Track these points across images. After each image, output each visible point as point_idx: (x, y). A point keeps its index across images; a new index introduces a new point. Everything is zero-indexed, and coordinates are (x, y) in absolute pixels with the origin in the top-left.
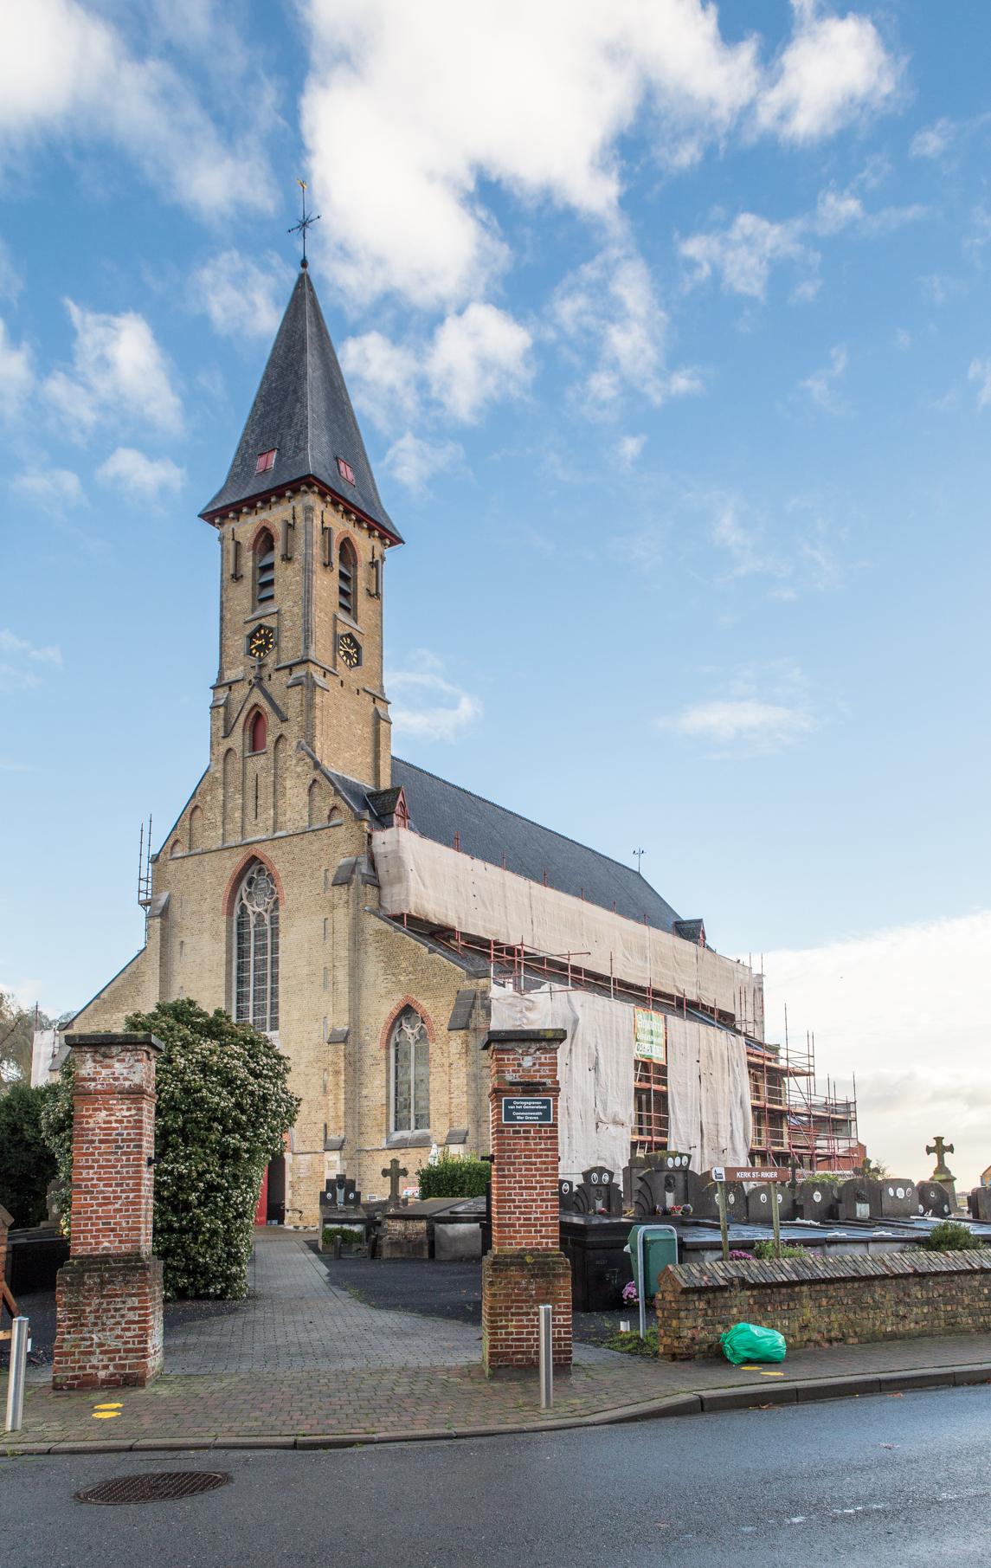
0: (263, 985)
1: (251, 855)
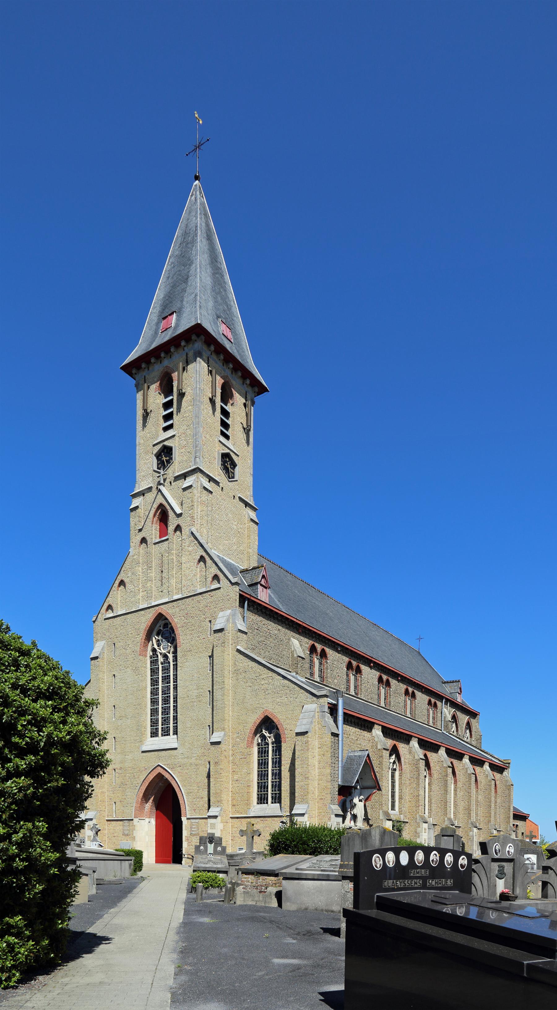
0: (167, 704)
1: (158, 612)
